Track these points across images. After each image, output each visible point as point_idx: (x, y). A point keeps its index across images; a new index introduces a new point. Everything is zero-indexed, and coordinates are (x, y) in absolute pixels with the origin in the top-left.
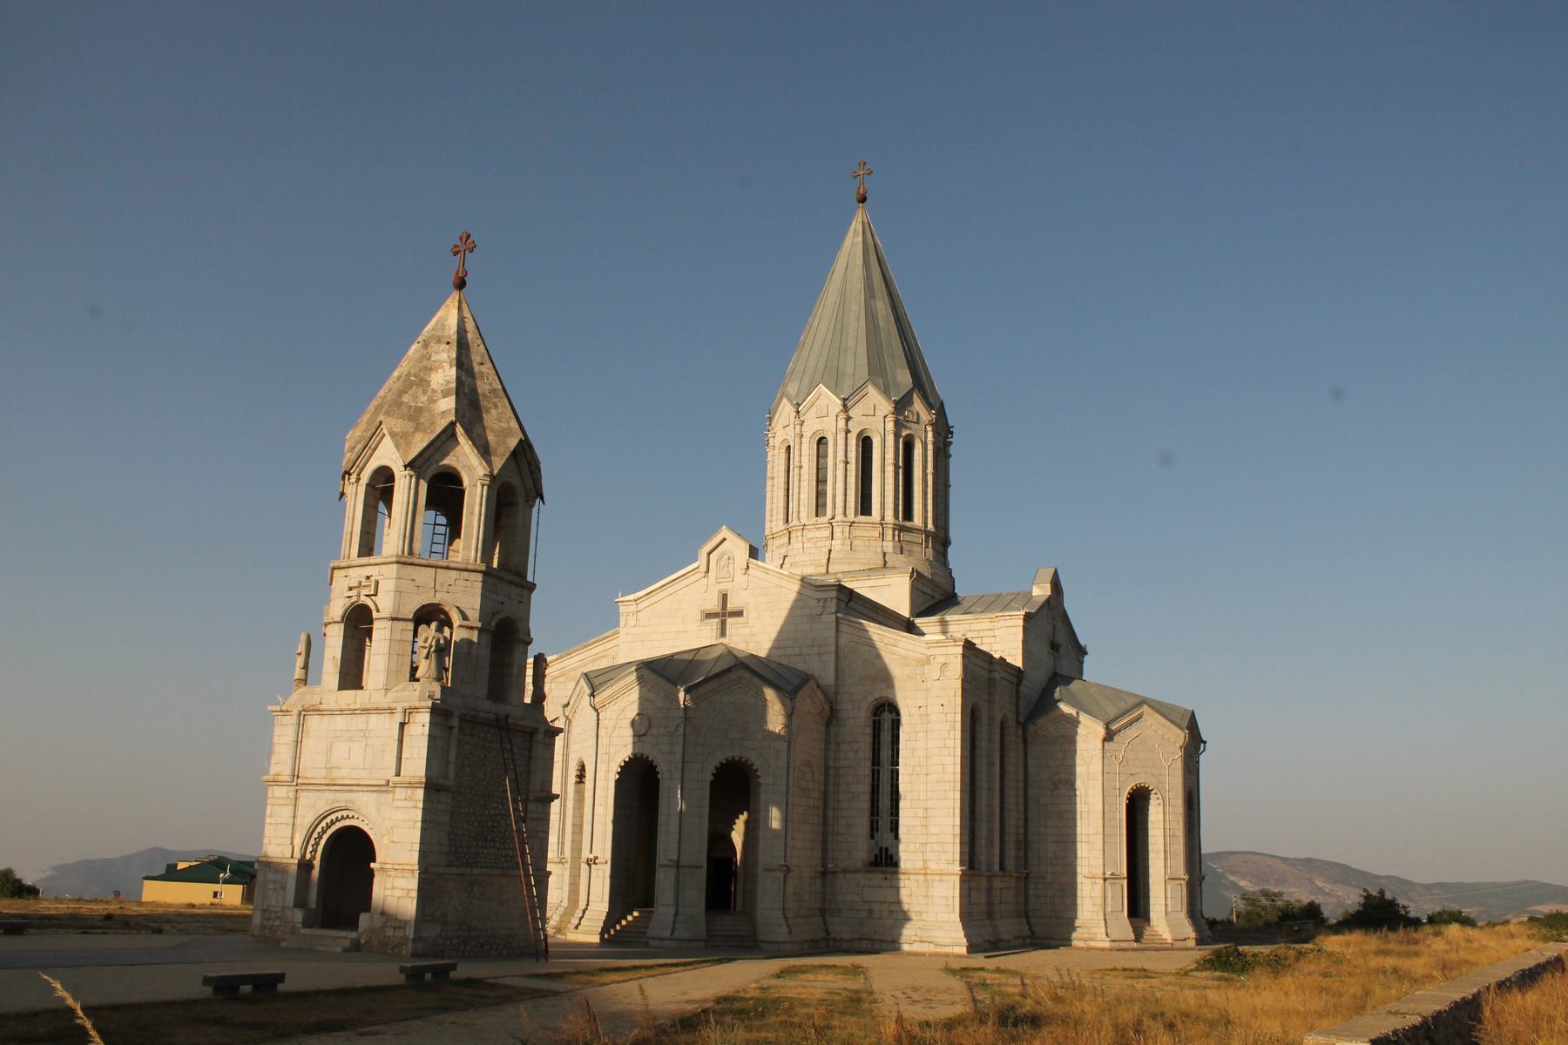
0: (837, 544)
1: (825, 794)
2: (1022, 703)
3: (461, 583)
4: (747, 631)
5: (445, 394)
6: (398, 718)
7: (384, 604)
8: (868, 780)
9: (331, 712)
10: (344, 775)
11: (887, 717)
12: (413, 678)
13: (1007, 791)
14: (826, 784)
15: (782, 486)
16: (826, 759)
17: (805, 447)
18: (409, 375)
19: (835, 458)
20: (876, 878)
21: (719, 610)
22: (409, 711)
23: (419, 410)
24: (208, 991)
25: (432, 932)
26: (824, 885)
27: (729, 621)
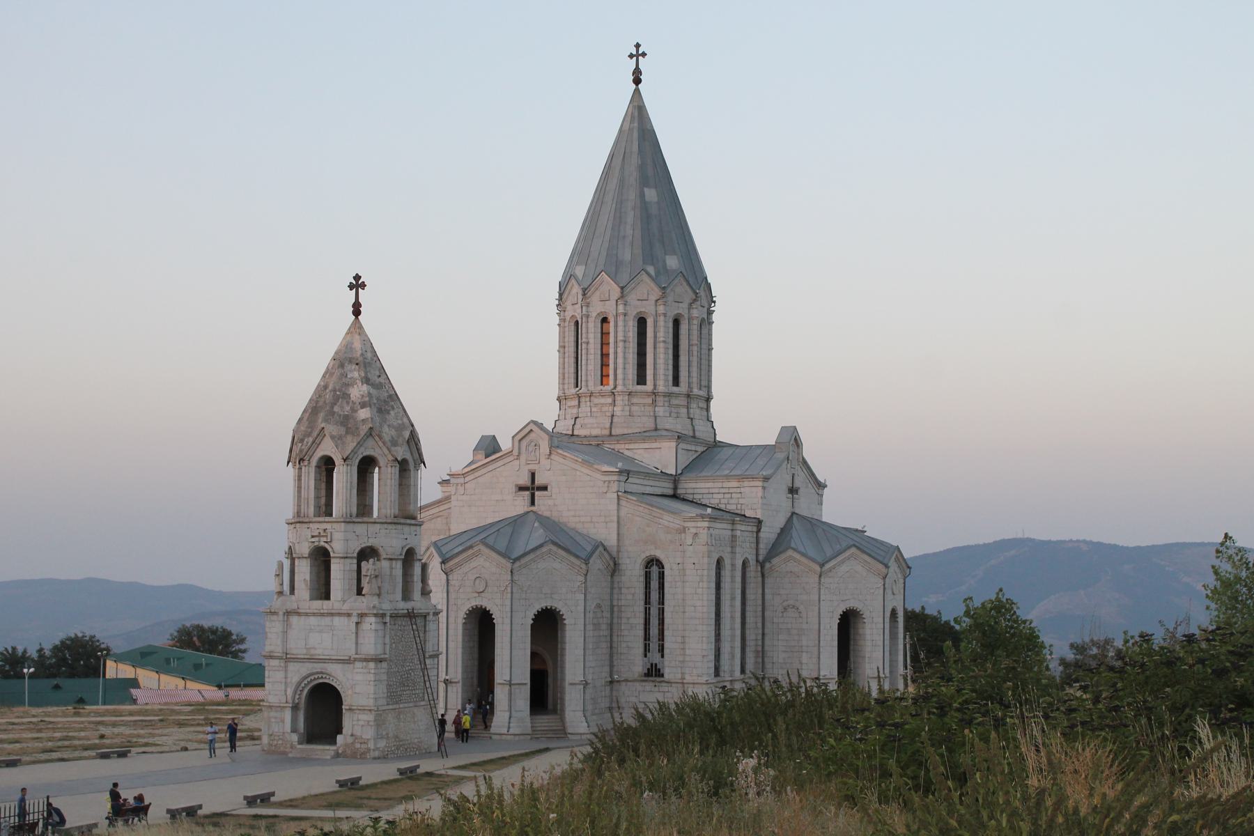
0: (618, 410)
1: (611, 625)
2: (761, 546)
3: (383, 531)
4: (550, 502)
5: (363, 405)
6: (355, 619)
7: (337, 547)
8: (642, 615)
9: (307, 614)
10: (319, 652)
11: (655, 569)
12: (359, 592)
13: (748, 614)
14: (612, 618)
15: (573, 355)
16: (611, 601)
17: (591, 325)
18: (335, 390)
19: (616, 337)
20: (649, 686)
21: (529, 484)
22: (362, 615)
23: (347, 417)
24: (336, 788)
25: (382, 744)
26: (611, 690)
27: (537, 493)
